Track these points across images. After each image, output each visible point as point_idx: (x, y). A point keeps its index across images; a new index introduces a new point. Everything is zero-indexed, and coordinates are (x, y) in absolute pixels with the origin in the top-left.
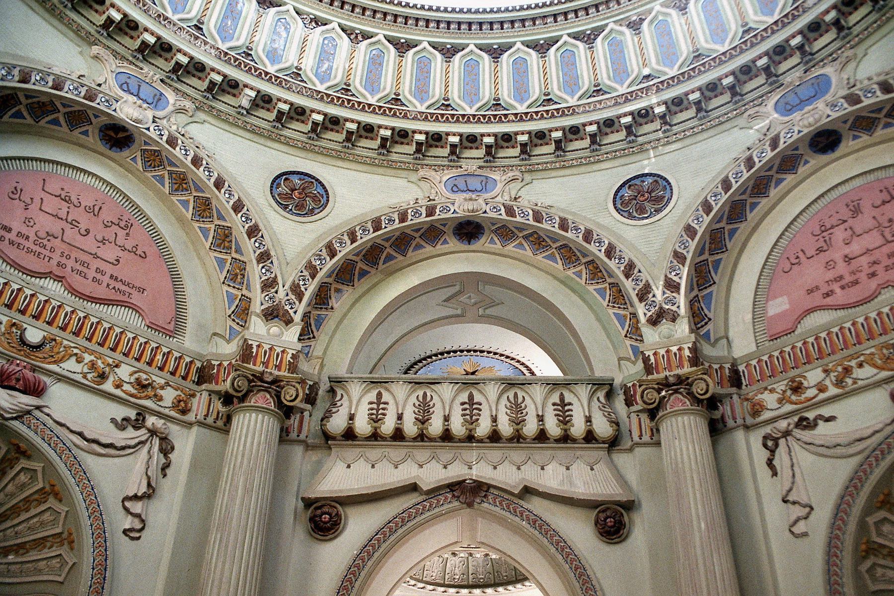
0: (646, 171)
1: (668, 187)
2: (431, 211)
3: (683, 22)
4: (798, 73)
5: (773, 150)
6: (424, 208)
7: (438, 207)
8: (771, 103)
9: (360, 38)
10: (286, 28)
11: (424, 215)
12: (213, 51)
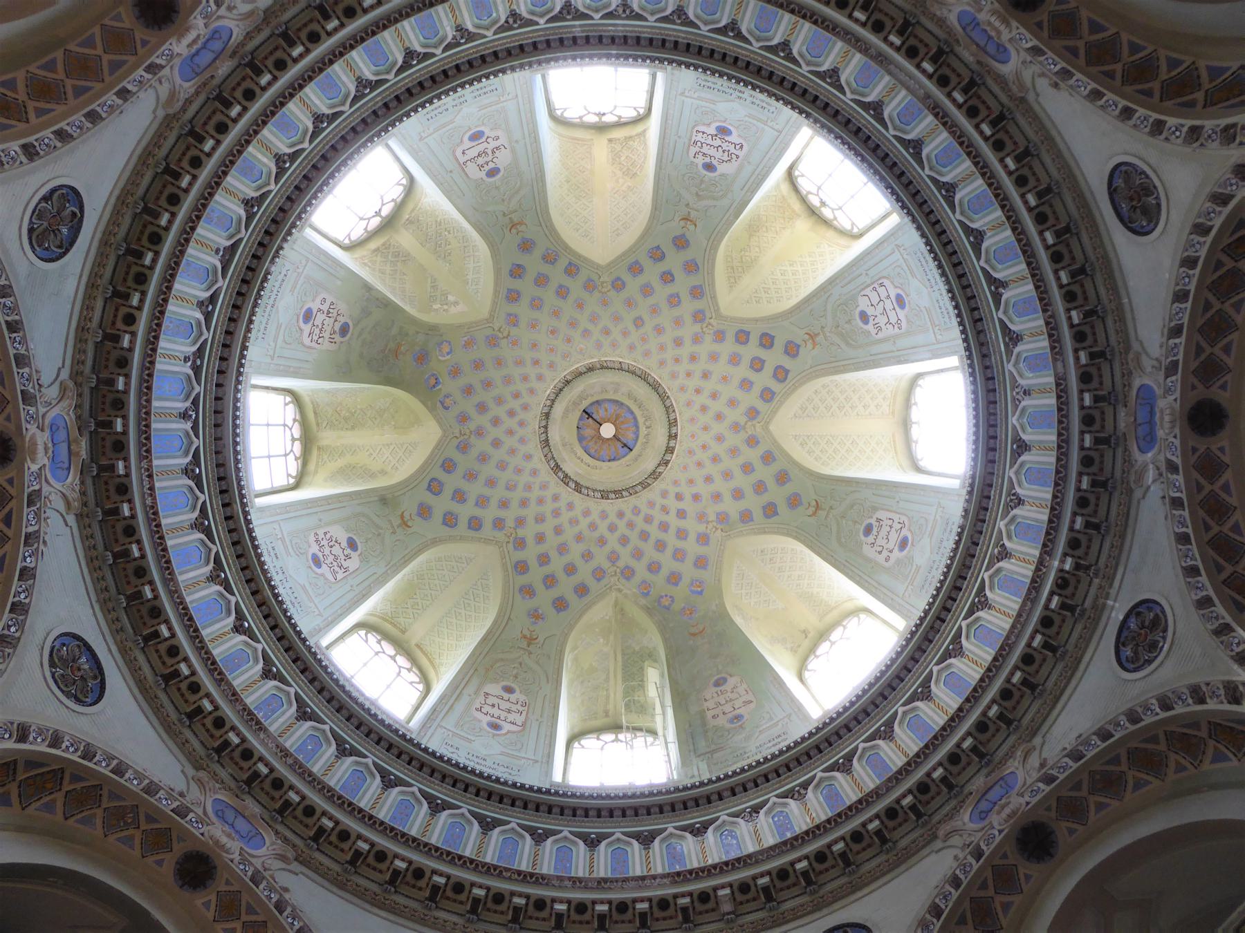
0: (1121, 618)
1: (1151, 605)
2: (978, 854)
3: (1029, 507)
4: (1122, 413)
5: (1178, 473)
6: (969, 857)
7: (982, 844)
8: (1136, 454)
9: (803, 791)
10: (732, 837)
11: (974, 862)
12: (665, 880)
